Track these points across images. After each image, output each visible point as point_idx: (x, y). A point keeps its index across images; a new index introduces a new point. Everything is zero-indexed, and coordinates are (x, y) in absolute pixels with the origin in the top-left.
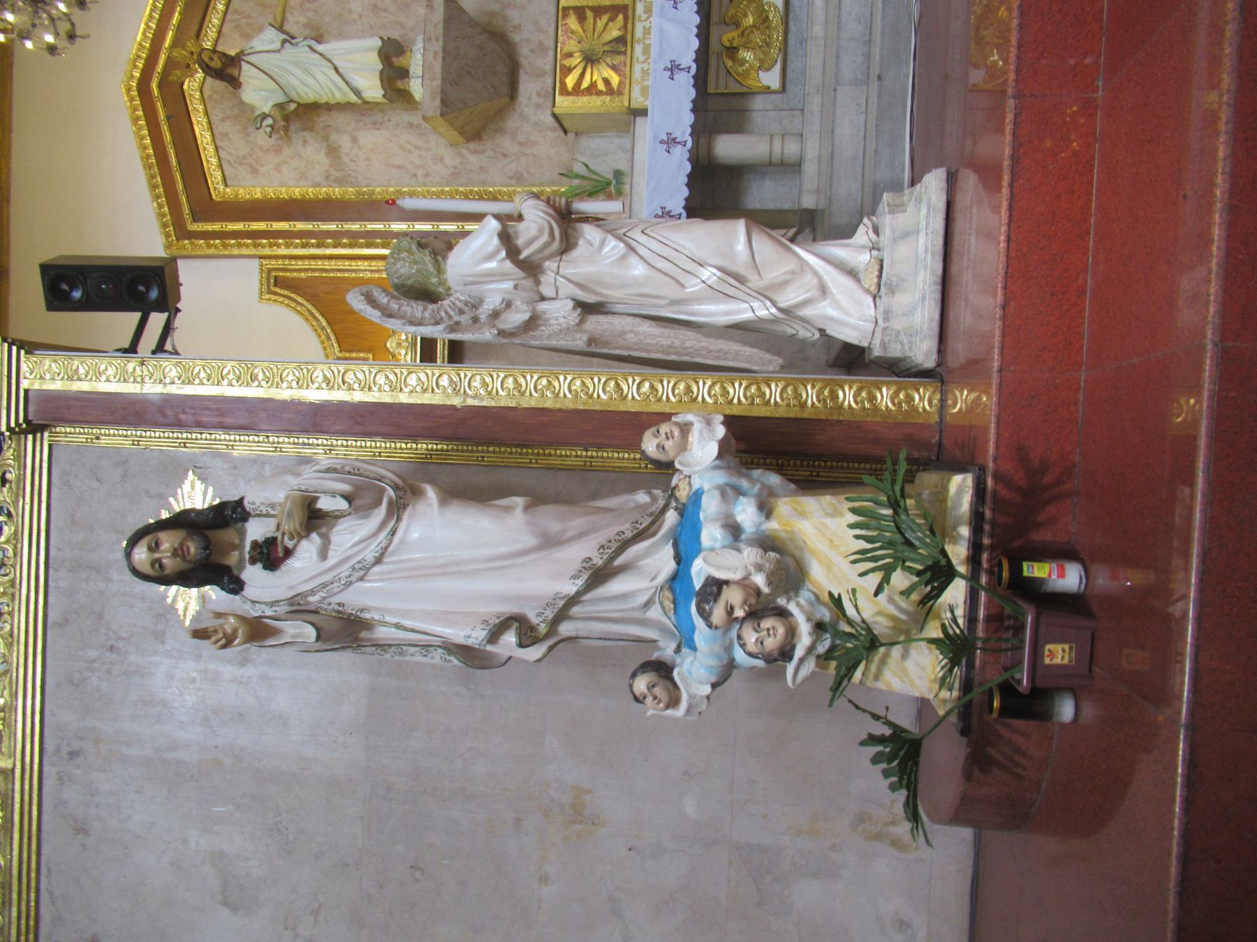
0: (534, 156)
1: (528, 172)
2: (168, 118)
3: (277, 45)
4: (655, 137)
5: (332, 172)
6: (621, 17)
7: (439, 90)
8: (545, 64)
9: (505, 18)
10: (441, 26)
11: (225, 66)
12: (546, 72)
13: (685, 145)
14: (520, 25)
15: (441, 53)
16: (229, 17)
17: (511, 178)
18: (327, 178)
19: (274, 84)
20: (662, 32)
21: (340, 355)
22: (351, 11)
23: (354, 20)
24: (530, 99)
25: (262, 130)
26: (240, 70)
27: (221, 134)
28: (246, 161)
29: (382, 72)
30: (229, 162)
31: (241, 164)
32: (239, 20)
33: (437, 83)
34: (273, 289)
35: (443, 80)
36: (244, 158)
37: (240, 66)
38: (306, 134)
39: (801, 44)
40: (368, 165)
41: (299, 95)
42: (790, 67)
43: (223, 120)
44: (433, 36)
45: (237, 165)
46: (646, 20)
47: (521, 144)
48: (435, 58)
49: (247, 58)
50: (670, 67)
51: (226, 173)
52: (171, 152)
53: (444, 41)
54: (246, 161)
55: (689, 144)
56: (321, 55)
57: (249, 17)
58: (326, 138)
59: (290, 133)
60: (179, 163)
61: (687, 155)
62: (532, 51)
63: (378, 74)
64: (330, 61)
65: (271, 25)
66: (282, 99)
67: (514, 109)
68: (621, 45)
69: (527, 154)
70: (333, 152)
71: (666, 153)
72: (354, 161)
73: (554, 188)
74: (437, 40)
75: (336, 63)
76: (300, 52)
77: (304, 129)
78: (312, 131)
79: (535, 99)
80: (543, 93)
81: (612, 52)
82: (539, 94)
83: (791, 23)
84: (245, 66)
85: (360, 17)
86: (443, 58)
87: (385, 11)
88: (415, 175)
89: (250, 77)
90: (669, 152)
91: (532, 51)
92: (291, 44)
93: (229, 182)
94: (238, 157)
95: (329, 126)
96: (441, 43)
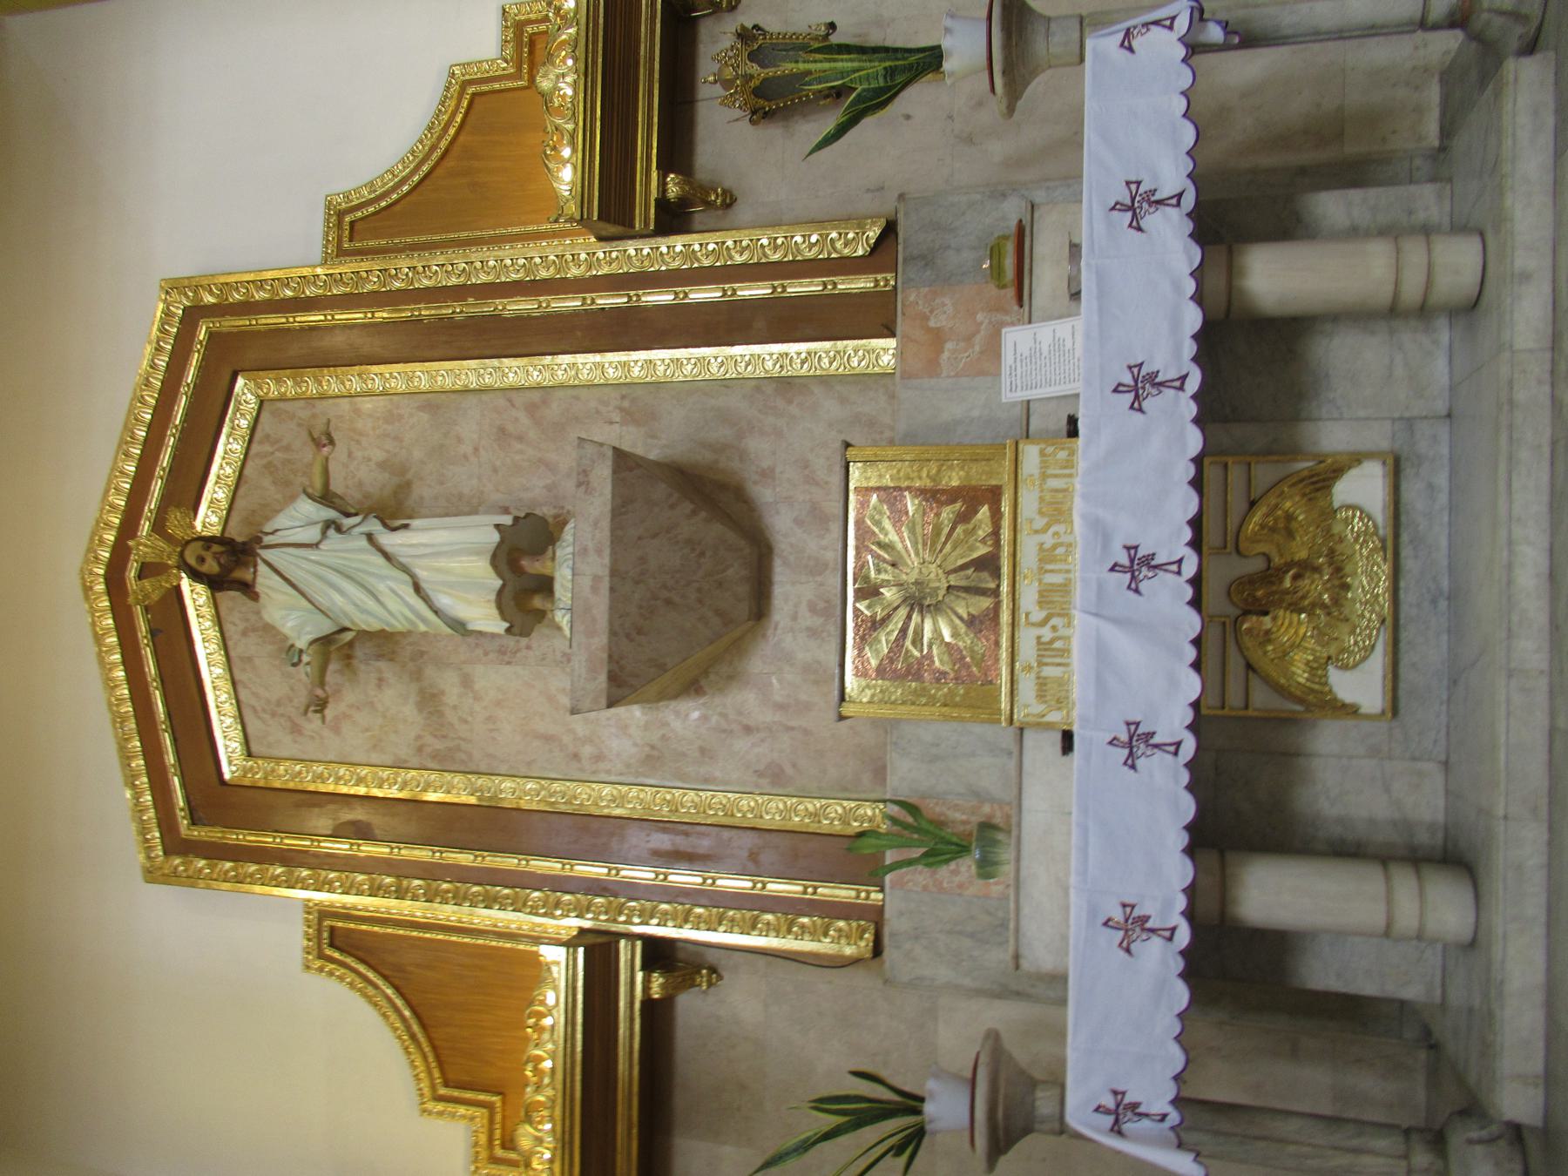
0: (806, 732)
1: (794, 765)
2: (153, 633)
3: (313, 534)
4: (1092, 911)
5: (429, 739)
6: (984, 511)
7: (605, 656)
8: (825, 548)
9: (743, 455)
10: (606, 524)
11: (226, 569)
12: (826, 566)
13: (1170, 939)
14: (772, 470)
15: (607, 579)
16: (255, 448)
17: (760, 774)
18: (420, 749)
19: (310, 606)
20: (1102, 654)
21: (442, 1091)
22: (459, 440)
23: (465, 457)
24: (795, 618)
25: (301, 667)
26: (255, 572)
27: (242, 659)
28: (281, 710)
29: (500, 593)
30: (255, 710)
31: (274, 715)
32: (272, 453)
33: (601, 640)
34: (329, 952)
35: (613, 633)
36: (279, 704)
37: (255, 566)
38: (382, 664)
39: (1434, 602)
40: (491, 731)
41: (352, 622)
42: (1405, 661)
43: (245, 633)
44: (590, 545)
45: (266, 716)
46: (1044, 531)
47: (781, 707)
48: (595, 589)
49: (266, 554)
50: (1124, 737)
51: (250, 730)
52: (158, 697)
53: (613, 553)
54: (281, 710)
55: (1184, 936)
56: (387, 556)
57: (287, 448)
58: (417, 676)
59: (355, 662)
60: (169, 714)
61: (1178, 964)
62: (798, 522)
63: (493, 597)
64: (405, 569)
65: (305, 492)
66: (326, 627)
67: (764, 636)
68: (985, 575)
69: (792, 729)
70: (429, 701)
71: (1122, 954)
72: (466, 722)
73: (845, 803)
74: (599, 552)
75: (422, 574)
76: (349, 549)
77: (379, 657)
78: (391, 660)
79: (808, 620)
80: (821, 605)
81: (967, 590)
82: (813, 609)
83: (1405, 552)
84: (262, 568)
85: (476, 450)
86: (612, 590)
87: (520, 438)
88: (576, 756)
89: (269, 587)
90: (1128, 950)
91: (798, 522)
92: (339, 529)
93: (254, 748)
94: (268, 702)
95: (422, 653)
96: (607, 560)
